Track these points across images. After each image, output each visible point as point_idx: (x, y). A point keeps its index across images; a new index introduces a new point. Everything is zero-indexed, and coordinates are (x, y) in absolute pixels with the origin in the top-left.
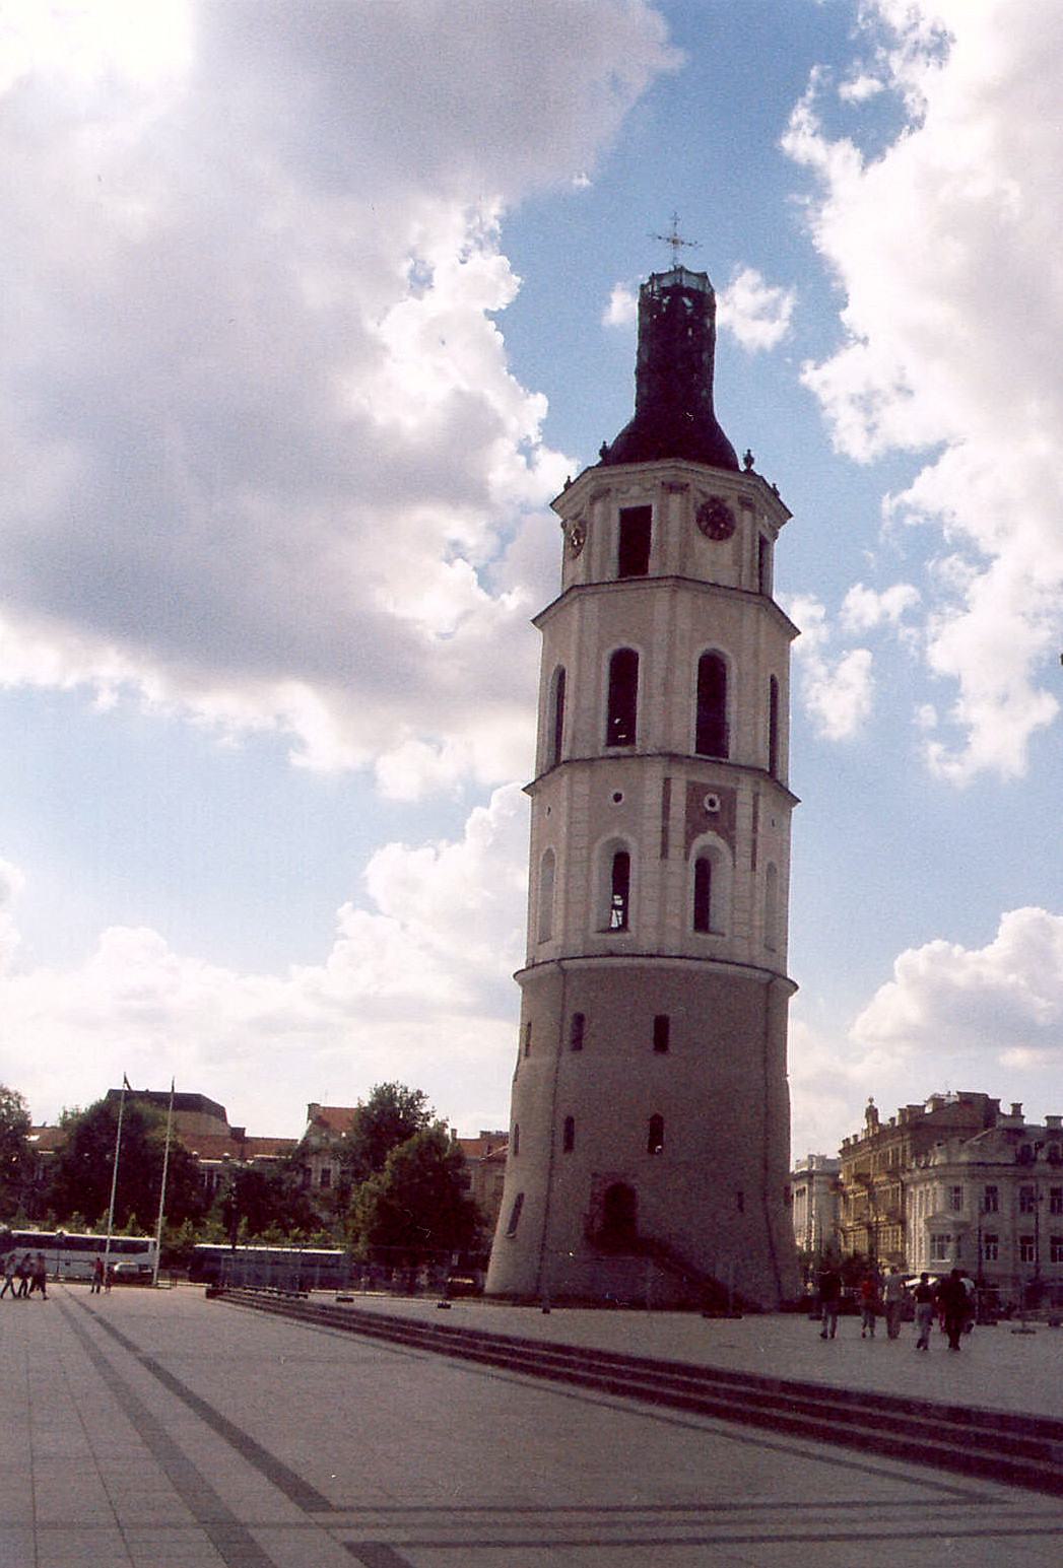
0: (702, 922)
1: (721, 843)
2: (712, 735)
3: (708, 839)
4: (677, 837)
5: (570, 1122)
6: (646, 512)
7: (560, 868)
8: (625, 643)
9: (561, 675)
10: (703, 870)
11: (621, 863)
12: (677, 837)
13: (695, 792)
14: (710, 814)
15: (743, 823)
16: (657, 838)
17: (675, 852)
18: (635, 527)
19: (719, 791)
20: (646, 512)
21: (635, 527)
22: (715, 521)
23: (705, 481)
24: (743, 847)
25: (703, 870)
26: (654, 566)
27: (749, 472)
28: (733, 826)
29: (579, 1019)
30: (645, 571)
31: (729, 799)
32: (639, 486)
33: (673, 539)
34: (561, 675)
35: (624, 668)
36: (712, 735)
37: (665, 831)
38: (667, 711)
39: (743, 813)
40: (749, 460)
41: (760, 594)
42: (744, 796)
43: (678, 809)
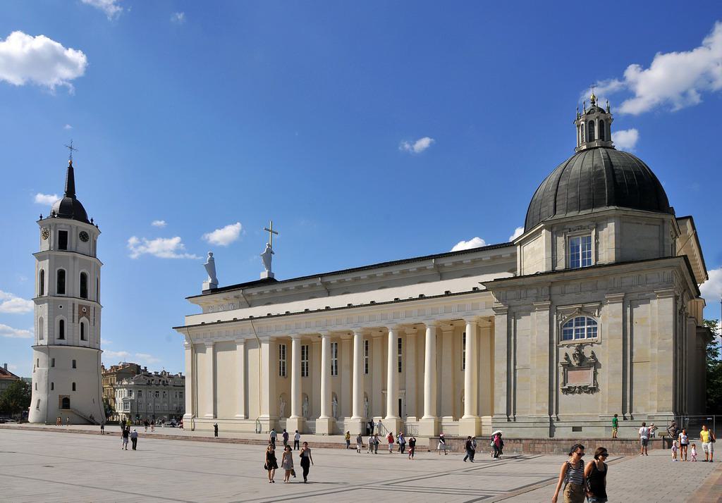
0: (82, 338)
2: (84, 294)
3: (84, 319)
4: (76, 318)
5: (53, 384)
6: (66, 233)
8: (61, 268)
10: (82, 324)
11: (62, 322)
12: (76, 318)
15: (92, 314)
16: (72, 318)
17: (76, 321)
19: (86, 307)
20: (66, 233)
22: (84, 236)
23: (82, 226)
25: (82, 324)
26: (68, 246)
27: (92, 224)
28: (89, 315)
29: (54, 360)
30: (66, 249)
31: (88, 308)
33: (74, 242)
35: (61, 274)
36: (84, 294)
37: (73, 316)
38: (73, 285)
39: (92, 312)
40: (92, 220)
41: (95, 257)
42: (92, 308)
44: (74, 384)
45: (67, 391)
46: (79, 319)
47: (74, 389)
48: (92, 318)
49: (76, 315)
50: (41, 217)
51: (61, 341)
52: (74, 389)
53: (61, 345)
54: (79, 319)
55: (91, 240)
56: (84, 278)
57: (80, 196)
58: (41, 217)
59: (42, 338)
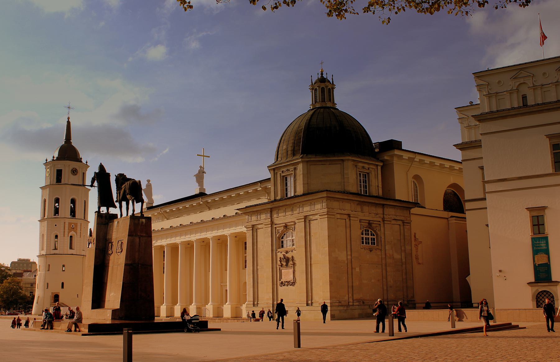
0: (71, 248)
1: (74, 233)
2: (73, 212)
3: (72, 233)
7: (45, 236)
9: (45, 201)
10: (71, 237)
13: (70, 224)
14: (73, 228)
17: (66, 235)
18: (59, 173)
19: (74, 224)
21: (59, 173)
22: (74, 172)
24: (79, 234)
25: (71, 237)
26: (63, 181)
31: (76, 224)
32: (61, 165)
34: (45, 201)
36: (73, 212)
42: (79, 225)
43: (67, 228)
44: (63, 284)
45: (57, 289)
46: (68, 233)
47: (63, 287)
48: (79, 231)
49: (67, 230)
50: (46, 160)
51: (55, 252)
52: (63, 287)
53: (55, 254)
54: (68, 233)
55: (80, 174)
56: (73, 201)
57: (74, 142)
58: (46, 160)
59: (43, 249)
